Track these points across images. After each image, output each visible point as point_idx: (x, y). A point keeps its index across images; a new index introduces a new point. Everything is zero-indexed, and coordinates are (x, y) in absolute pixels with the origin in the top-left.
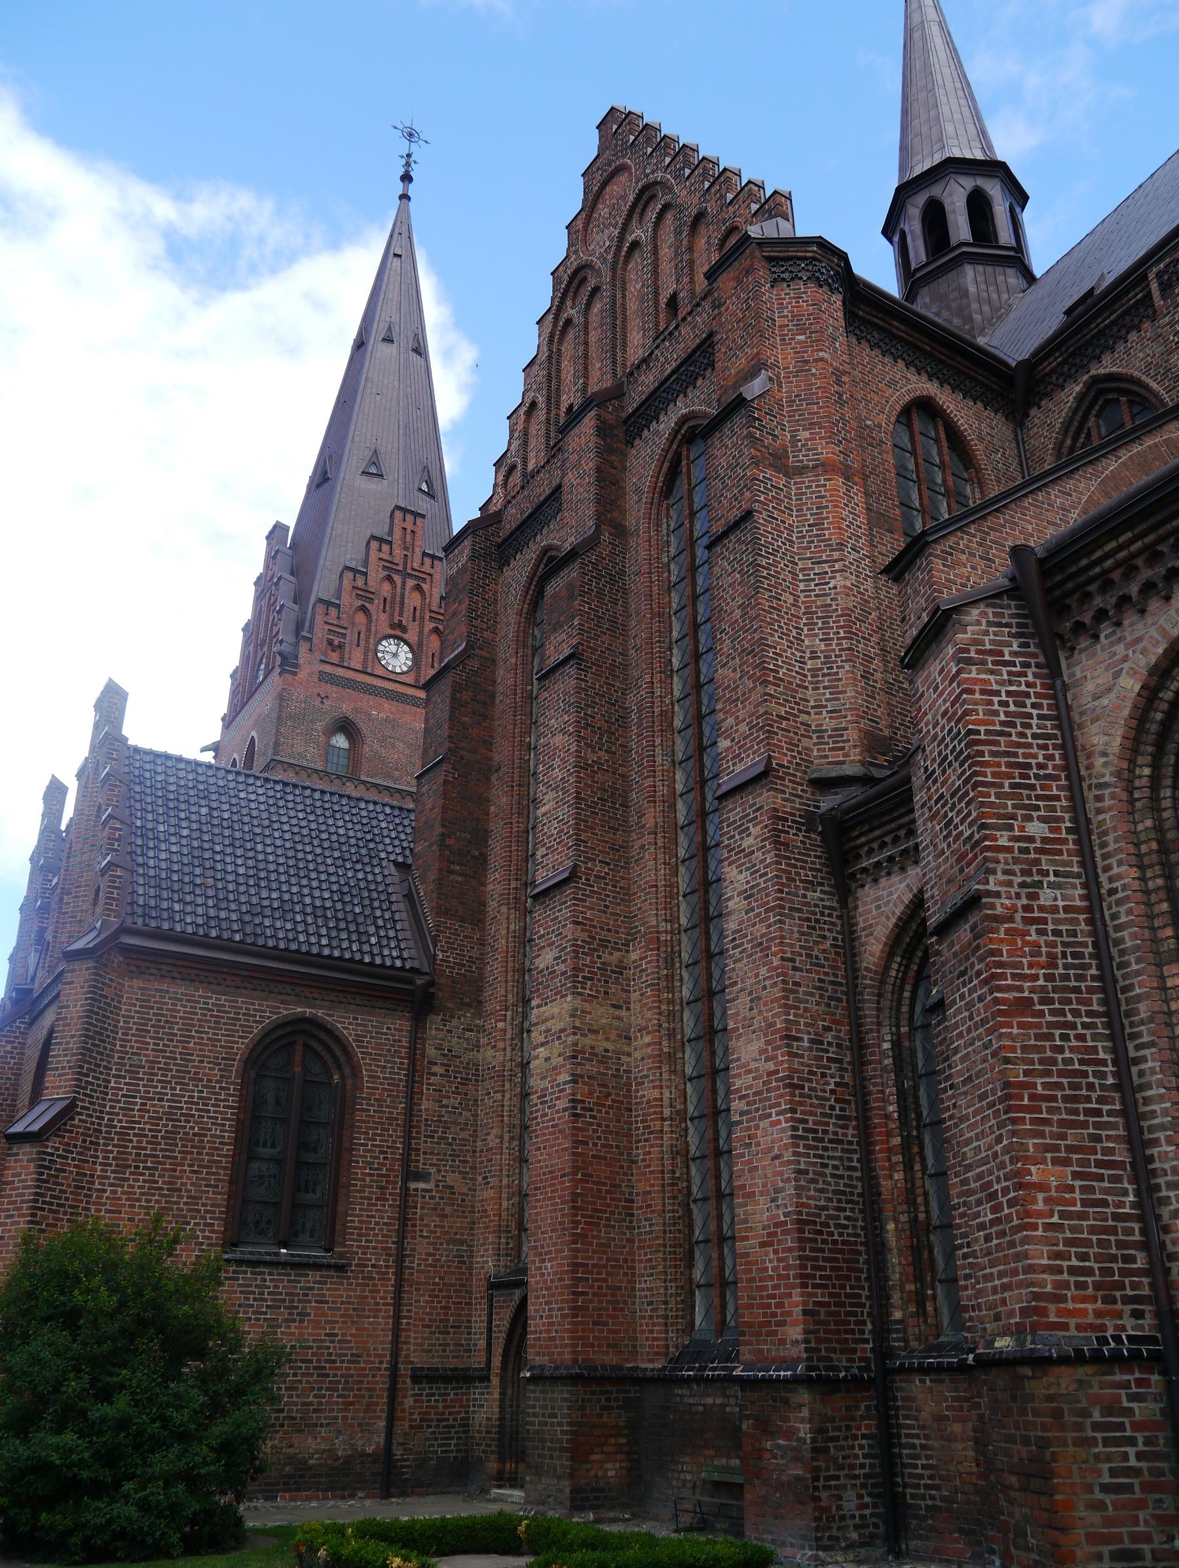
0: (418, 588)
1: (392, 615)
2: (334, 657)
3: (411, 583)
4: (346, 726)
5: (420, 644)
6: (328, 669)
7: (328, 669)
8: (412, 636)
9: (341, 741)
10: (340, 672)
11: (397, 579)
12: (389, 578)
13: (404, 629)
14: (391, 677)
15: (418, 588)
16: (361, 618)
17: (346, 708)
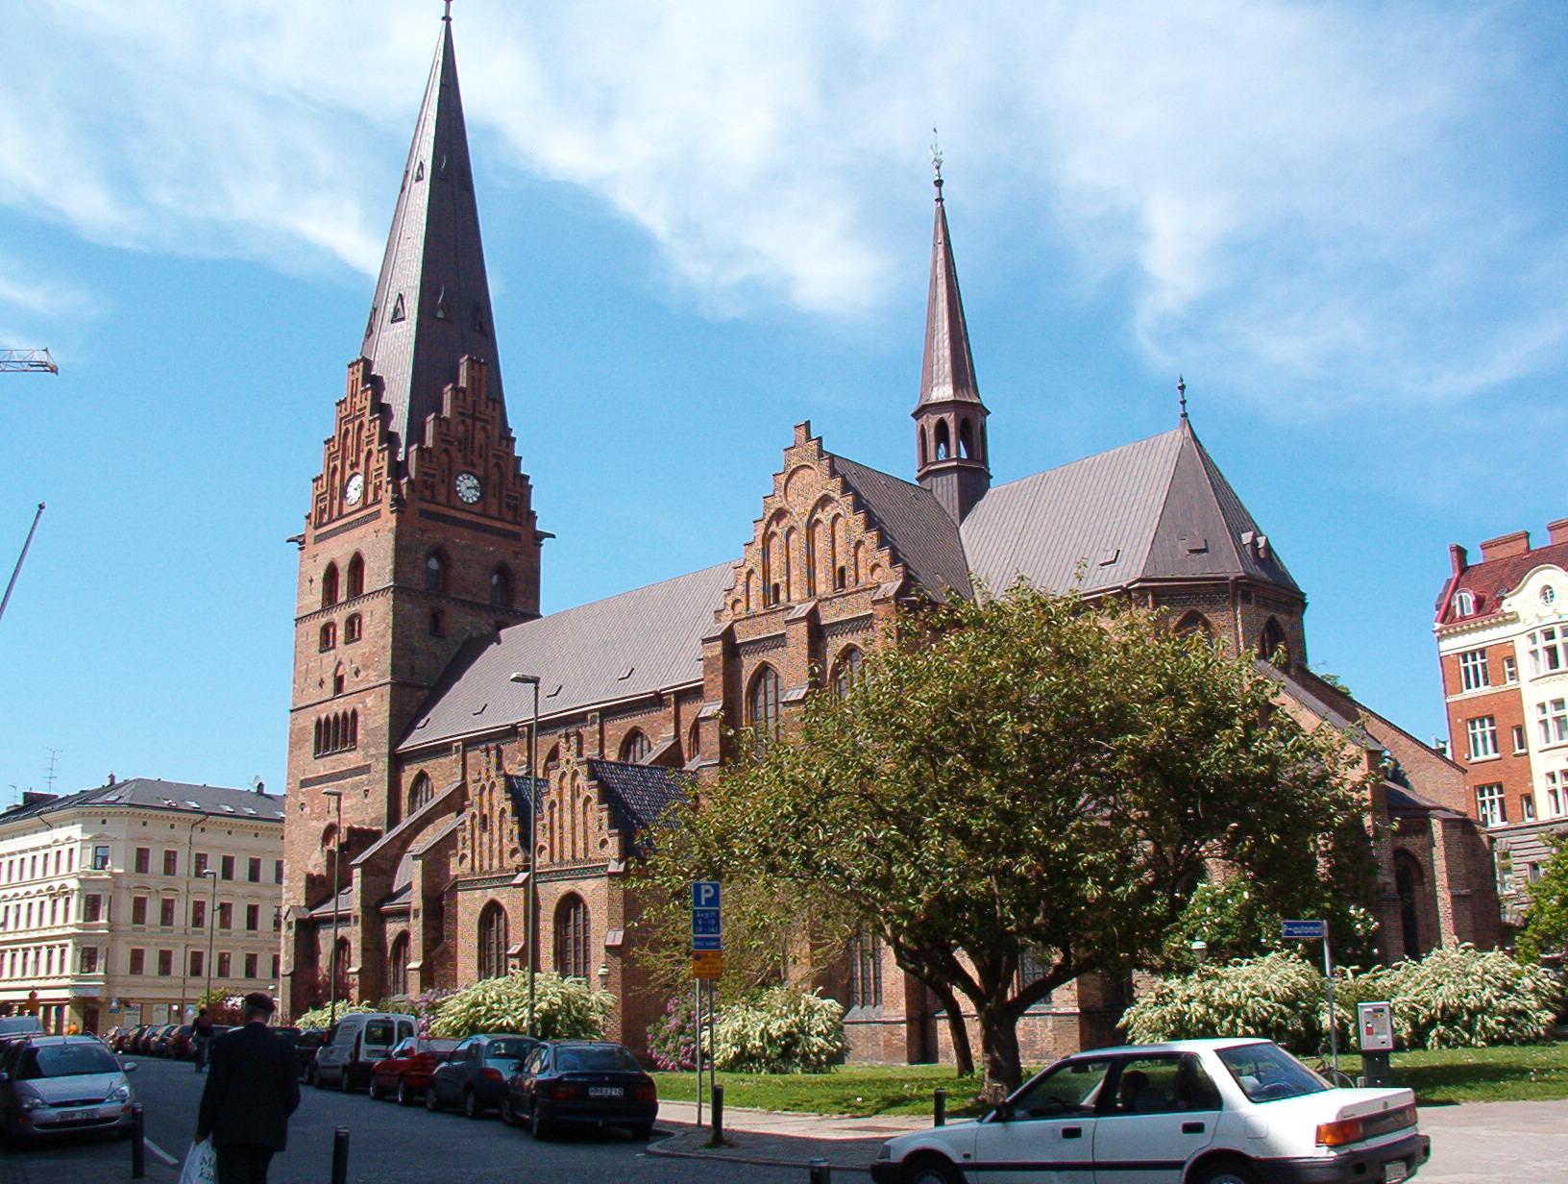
0: (484, 429)
1: (465, 457)
2: (427, 493)
3: (479, 425)
4: (439, 553)
5: (486, 477)
6: (426, 506)
7: (426, 506)
8: (480, 472)
9: (433, 564)
10: (433, 507)
11: (469, 422)
12: (463, 422)
13: (473, 464)
14: (466, 507)
15: (484, 429)
16: (444, 459)
17: (439, 538)
